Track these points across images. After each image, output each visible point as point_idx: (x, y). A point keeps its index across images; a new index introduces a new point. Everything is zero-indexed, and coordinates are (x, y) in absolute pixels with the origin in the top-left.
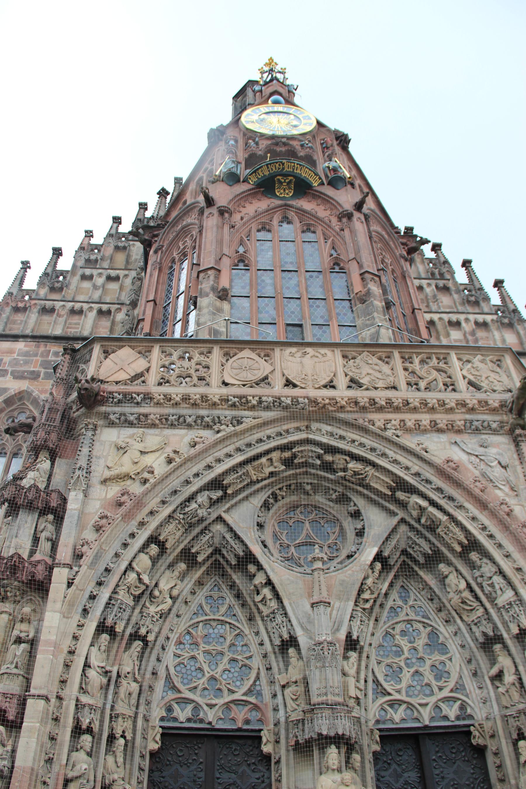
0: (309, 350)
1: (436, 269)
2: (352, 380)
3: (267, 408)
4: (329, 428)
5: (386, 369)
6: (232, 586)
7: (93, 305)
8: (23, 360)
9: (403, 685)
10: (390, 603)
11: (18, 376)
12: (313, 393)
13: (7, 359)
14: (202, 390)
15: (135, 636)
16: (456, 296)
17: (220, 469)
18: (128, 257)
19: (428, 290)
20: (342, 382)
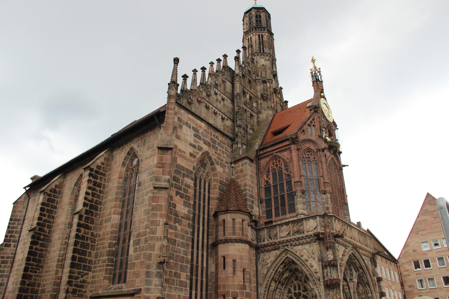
11: (205, 143)
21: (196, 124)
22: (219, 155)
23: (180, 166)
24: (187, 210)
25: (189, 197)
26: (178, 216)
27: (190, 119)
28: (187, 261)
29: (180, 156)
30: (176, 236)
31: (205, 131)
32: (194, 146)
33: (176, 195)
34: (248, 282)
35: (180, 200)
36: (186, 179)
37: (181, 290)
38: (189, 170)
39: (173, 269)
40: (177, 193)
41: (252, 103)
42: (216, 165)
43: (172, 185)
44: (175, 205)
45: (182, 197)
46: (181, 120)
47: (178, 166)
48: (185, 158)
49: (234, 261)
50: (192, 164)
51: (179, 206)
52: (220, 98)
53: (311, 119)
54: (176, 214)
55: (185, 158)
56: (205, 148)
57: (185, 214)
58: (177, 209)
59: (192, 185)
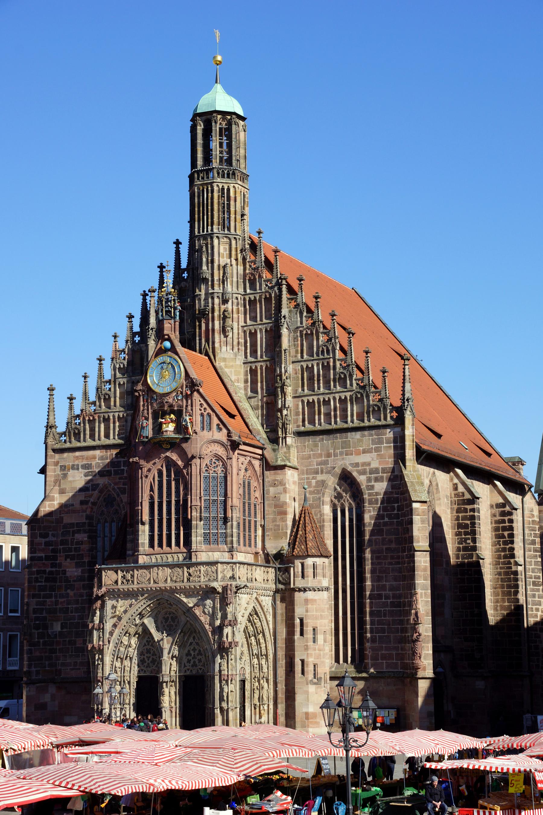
4: (167, 594)
9: (191, 664)
10: (190, 641)
13: (94, 463)
14: (132, 586)
15: (127, 657)
17: (140, 610)
21: (87, 459)
24: (80, 570)
25: (82, 554)
26: (70, 581)
27: (77, 458)
29: (67, 513)
30: (68, 604)
33: (66, 560)
36: (76, 535)
40: (67, 557)
42: (121, 496)
43: (60, 550)
44: (65, 571)
45: (72, 558)
46: (65, 467)
47: (65, 526)
48: (74, 512)
50: (85, 514)
51: (70, 570)
54: (67, 580)
55: (74, 512)
58: (68, 574)
59: (86, 539)
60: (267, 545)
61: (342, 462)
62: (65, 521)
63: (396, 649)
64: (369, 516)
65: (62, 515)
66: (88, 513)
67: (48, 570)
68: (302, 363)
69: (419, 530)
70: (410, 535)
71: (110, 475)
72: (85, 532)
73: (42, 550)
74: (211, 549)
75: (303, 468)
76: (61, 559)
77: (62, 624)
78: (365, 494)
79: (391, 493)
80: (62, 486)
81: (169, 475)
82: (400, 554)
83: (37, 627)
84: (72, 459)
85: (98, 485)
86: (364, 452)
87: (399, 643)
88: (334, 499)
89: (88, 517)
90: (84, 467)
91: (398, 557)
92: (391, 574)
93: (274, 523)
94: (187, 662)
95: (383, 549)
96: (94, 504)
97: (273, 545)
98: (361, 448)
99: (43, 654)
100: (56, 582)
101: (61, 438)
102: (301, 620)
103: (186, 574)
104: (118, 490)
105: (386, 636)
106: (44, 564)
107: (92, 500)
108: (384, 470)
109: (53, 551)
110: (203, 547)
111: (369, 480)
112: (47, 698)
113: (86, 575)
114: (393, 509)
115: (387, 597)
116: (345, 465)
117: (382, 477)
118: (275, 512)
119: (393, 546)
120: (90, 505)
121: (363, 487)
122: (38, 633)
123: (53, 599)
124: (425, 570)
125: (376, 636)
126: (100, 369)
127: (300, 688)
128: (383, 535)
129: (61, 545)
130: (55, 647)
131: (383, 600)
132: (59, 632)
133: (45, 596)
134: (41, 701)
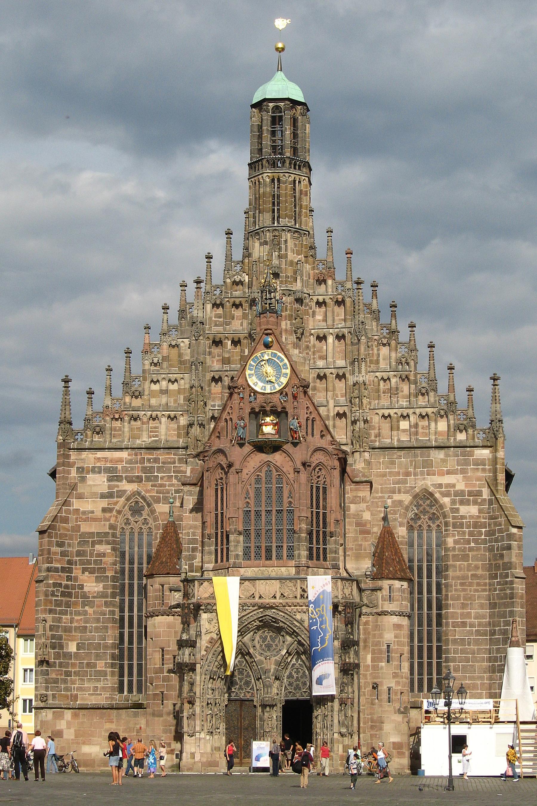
0: (268, 581)
1: (403, 358)
2: (282, 594)
3: (253, 606)
5: (294, 589)
6: (245, 659)
7: (164, 413)
8: (130, 467)
10: (292, 663)
11: (130, 480)
12: (267, 601)
13: (119, 467)
15: (219, 677)
16: (413, 386)
18: (180, 355)
19: (393, 381)
20: (278, 595)
21: (111, 461)
22: (161, 485)
23: (86, 533)
24: (101, 585)
25: (105, 568)
26: (89, 597)
28: (106, 647)
30: (86, 622)
31: (130, 462)
32: (110, 495)
33: (83, 573)
34: (167, 664)
35: (89, 577)
36: (97, 546)
37: (99, 680)
38: (102, 533)
39: (84, 659)
40: (84, 570)
41: (243, 351)
42: (155, 505)
43: (76, 562)
46: (83, 468)
47: (83, 535)
49: (152, 639)
51: (88, 584)
52: (164, 383)
53: (228, 409)
54: (85, 596)
56: (130, 488)
57: (98, 592)
58: (86, 589)
59: (110, 551)
60: (348, 567)
61: (423, 482)
62: (82, 530)
63: (482, 678)
64: (452, 540)
65: (79, 523)
66: (112, 521)
67: (64, 582)
68: (377, 374)
69: (516, 556)
70: (506, 560)
71: (141, 481)
72: (108, 543)
73: (58, 561)
74: (316, 564)
75: (377, 486)
76: (77, 572)
77: (78, 644)
78: (449, 518)
79: (479, 517)
80: (80, 490)
81: (269, 481)
82: (487, 581)
83: (53, 647)
84: (92, 460)
85: (125, 491)
86: (449, 473)
87: (485, 672)
88: (410, 522)
89: (112, 527)
90: (108, 470)
91: (485, 584)
92: (477, 602)
93: (356, 543)
94: (289, 685)
95: (468, 576)
96: (119, 512)
97: (354, 566)
98: (445, 469)
99: (59, 677)
100: (71, 598)
101: (76, 437)
102: (388, 646)
103: (299, 591)
104: (150, 499)
105: (470, 665)
106: (60, 576)
107: (117, 507)
108: (470, 494)
109: (70, 562)
110: (310, 563)
111: (453, 502)
112: (62, 725)
113: (109, 591)
114: (480, 534)
115: (472, 625)
116: (427, 485)
117: (469, 500)
118: (356, 530)
119: (480, 572)
120: (114, 513)
121: (447, 509)
122: (54, 653)
123: (69, 617)
124: (522, 597)
125: (459, 665)
126: (128, 363)
127: (388, 717)
128: (468, 561)
129: (77, 556)
130: (70, 670)
131: (468, 628)
132: (75, 653)
133: (62, 613)
134: (58, 728)
